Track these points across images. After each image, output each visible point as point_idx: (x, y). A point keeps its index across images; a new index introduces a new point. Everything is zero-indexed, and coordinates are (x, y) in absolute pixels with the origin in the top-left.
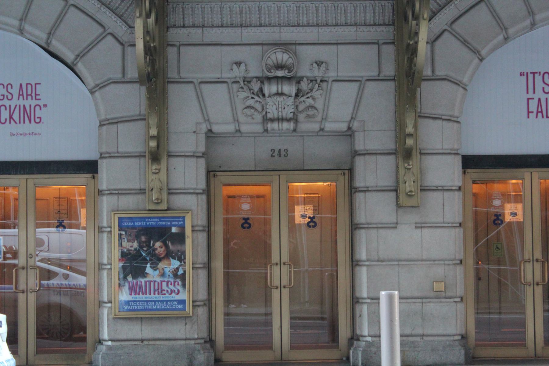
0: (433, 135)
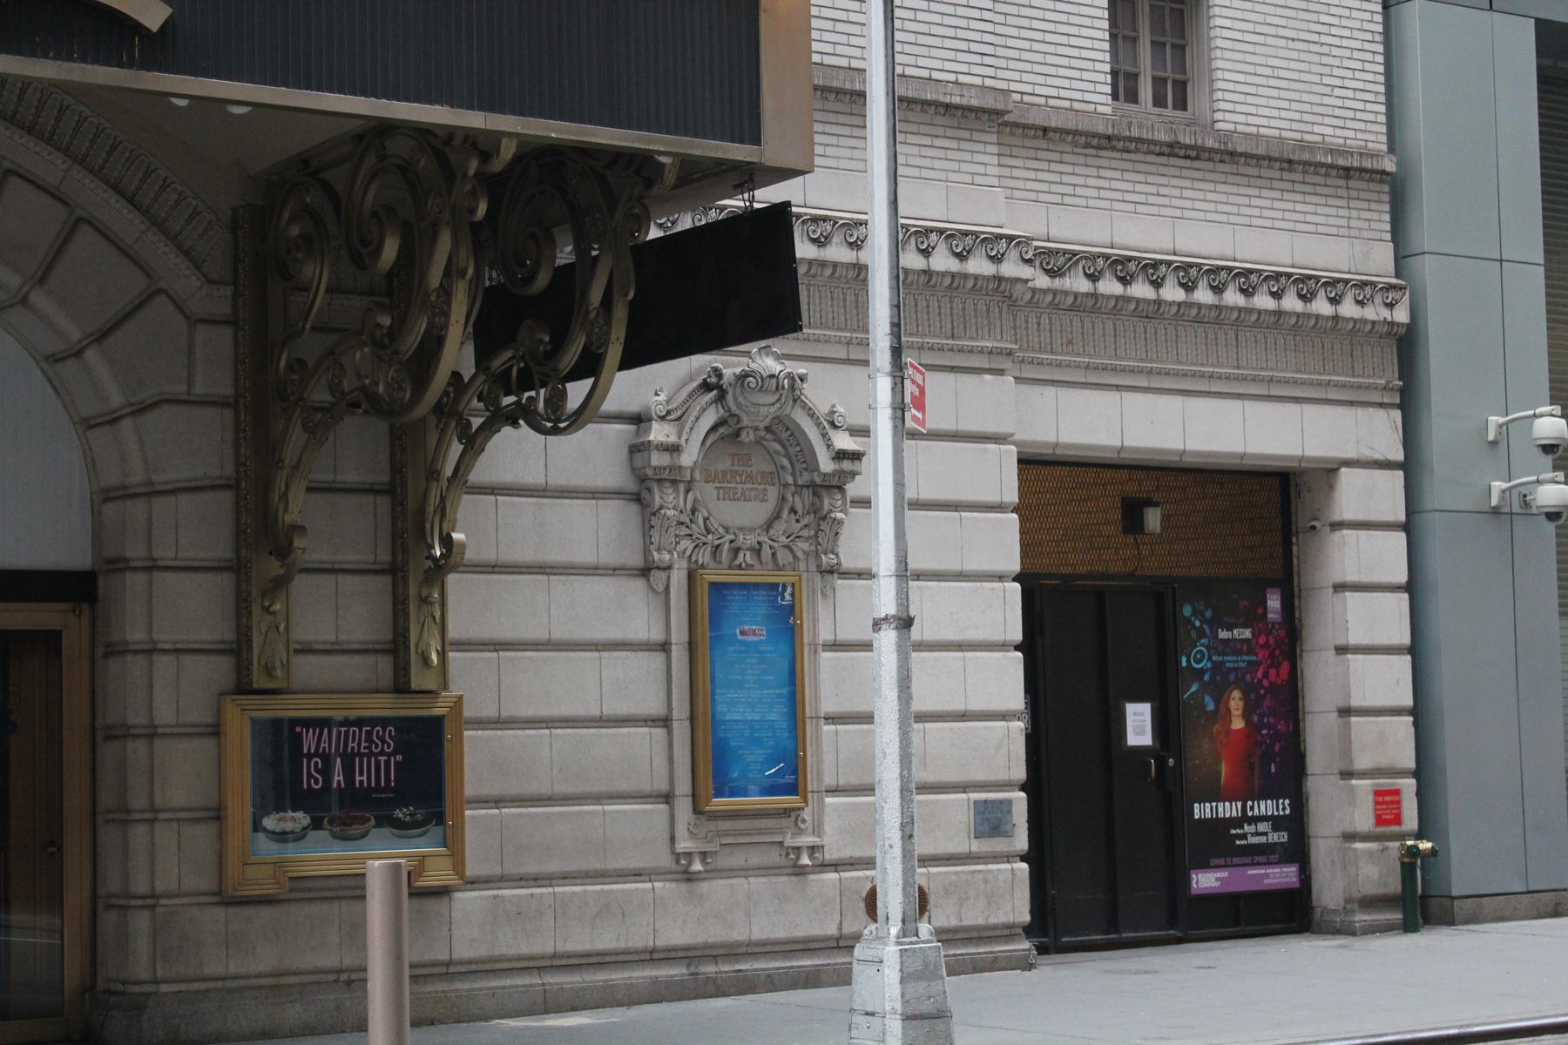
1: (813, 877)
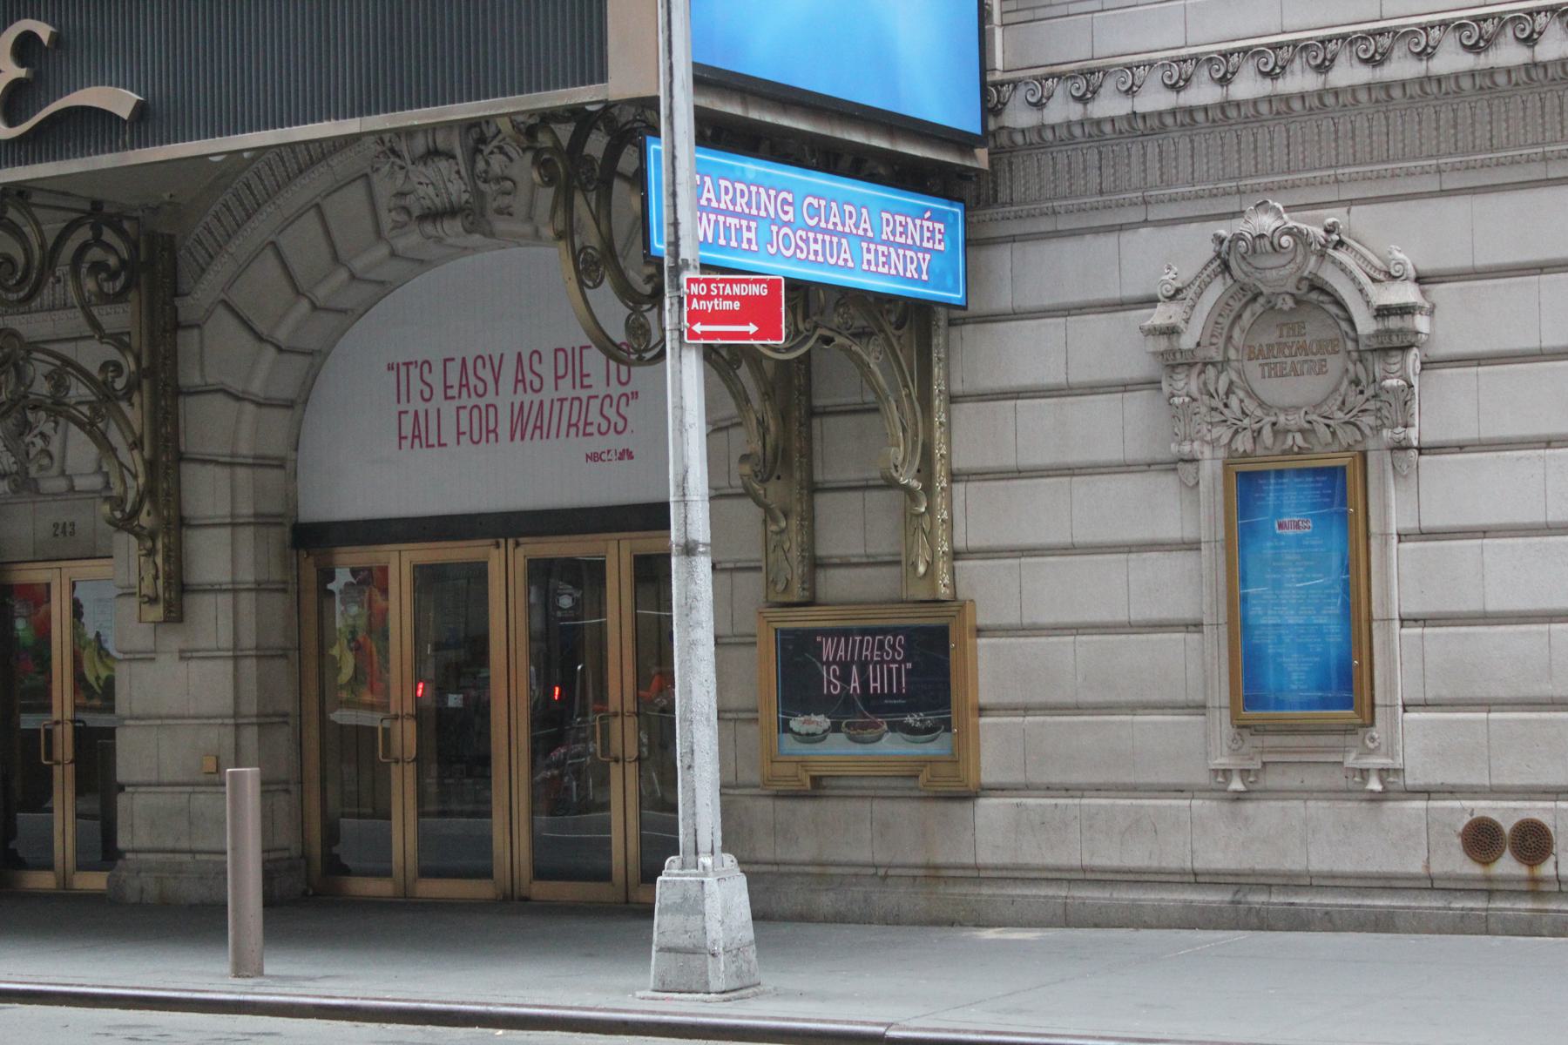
0: (207, 492)
1: (1390, 804)
